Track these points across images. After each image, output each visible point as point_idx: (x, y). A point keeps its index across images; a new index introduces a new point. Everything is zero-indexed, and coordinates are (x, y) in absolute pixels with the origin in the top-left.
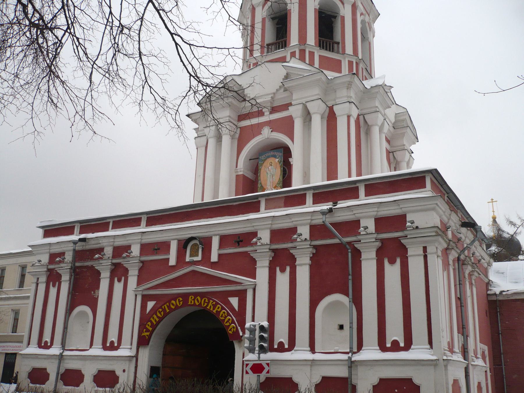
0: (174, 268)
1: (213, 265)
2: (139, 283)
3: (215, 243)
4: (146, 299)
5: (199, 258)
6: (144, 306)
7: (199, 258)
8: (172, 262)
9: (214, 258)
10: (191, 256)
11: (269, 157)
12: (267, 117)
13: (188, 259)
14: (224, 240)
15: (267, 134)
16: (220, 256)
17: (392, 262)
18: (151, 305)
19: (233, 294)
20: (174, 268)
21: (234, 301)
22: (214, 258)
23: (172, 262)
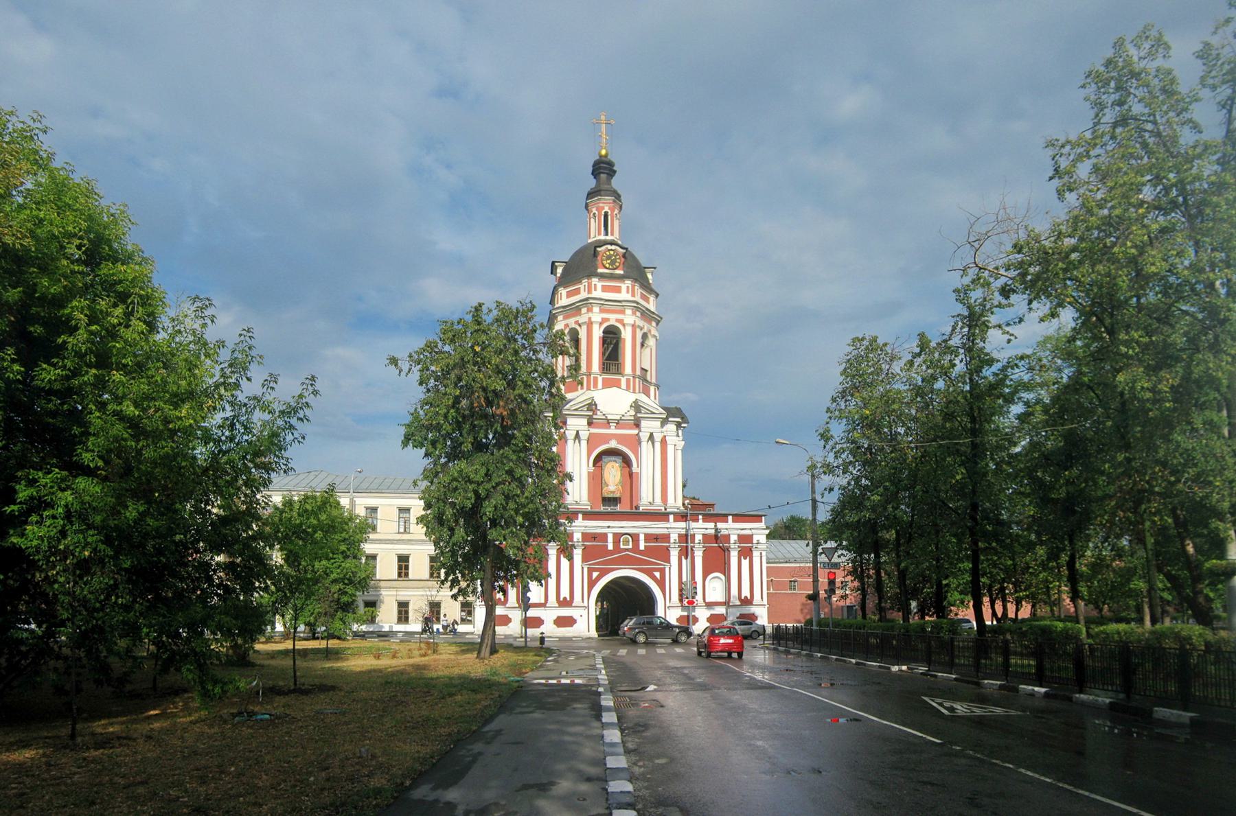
0: (612, 553)
1: (641, 552)
2: (585, 559)
3: (642, 537)
4: (590, 571)
5: (630, 547)
6: (590, 575)
7: (630, 547)
8: (610, 547)
9: (642, 547)
10: (623, 545)
11: (611, 461)
12: (613, 430)
13: (622, 547)
14: (649, 538)
15: (613, 444)
16: (645, 546)
17: (745, 558)
18: (595, 574)
19: (657, 570)
20: (612, 553)
21: (657, 574)
22: (642, 547)
23: (610, 547)
